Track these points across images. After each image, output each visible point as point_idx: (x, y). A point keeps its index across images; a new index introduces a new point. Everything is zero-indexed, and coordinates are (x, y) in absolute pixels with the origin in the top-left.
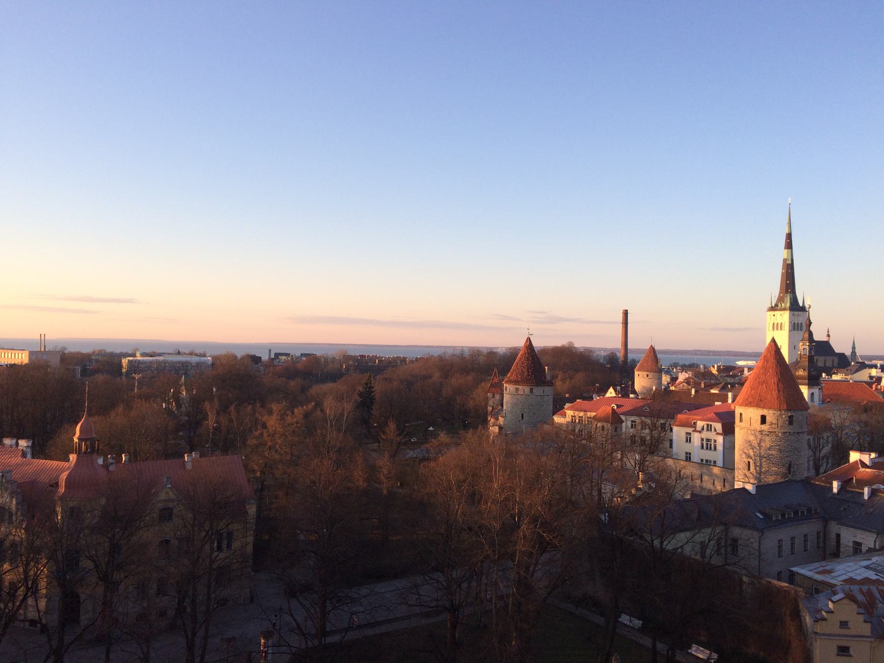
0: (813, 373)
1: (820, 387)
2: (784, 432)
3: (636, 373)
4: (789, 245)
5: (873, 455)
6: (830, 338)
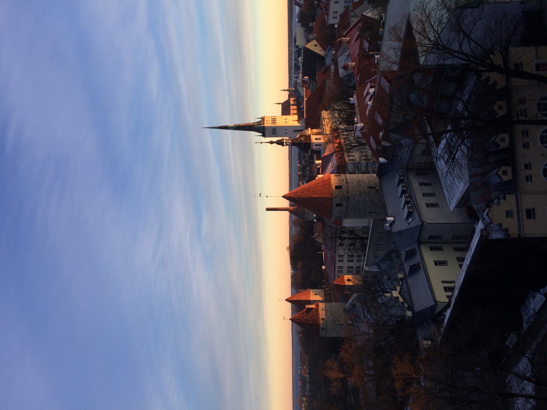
1: (311, 135)
2: (347, 192)
3: (306, 220)
6: (280, 102)
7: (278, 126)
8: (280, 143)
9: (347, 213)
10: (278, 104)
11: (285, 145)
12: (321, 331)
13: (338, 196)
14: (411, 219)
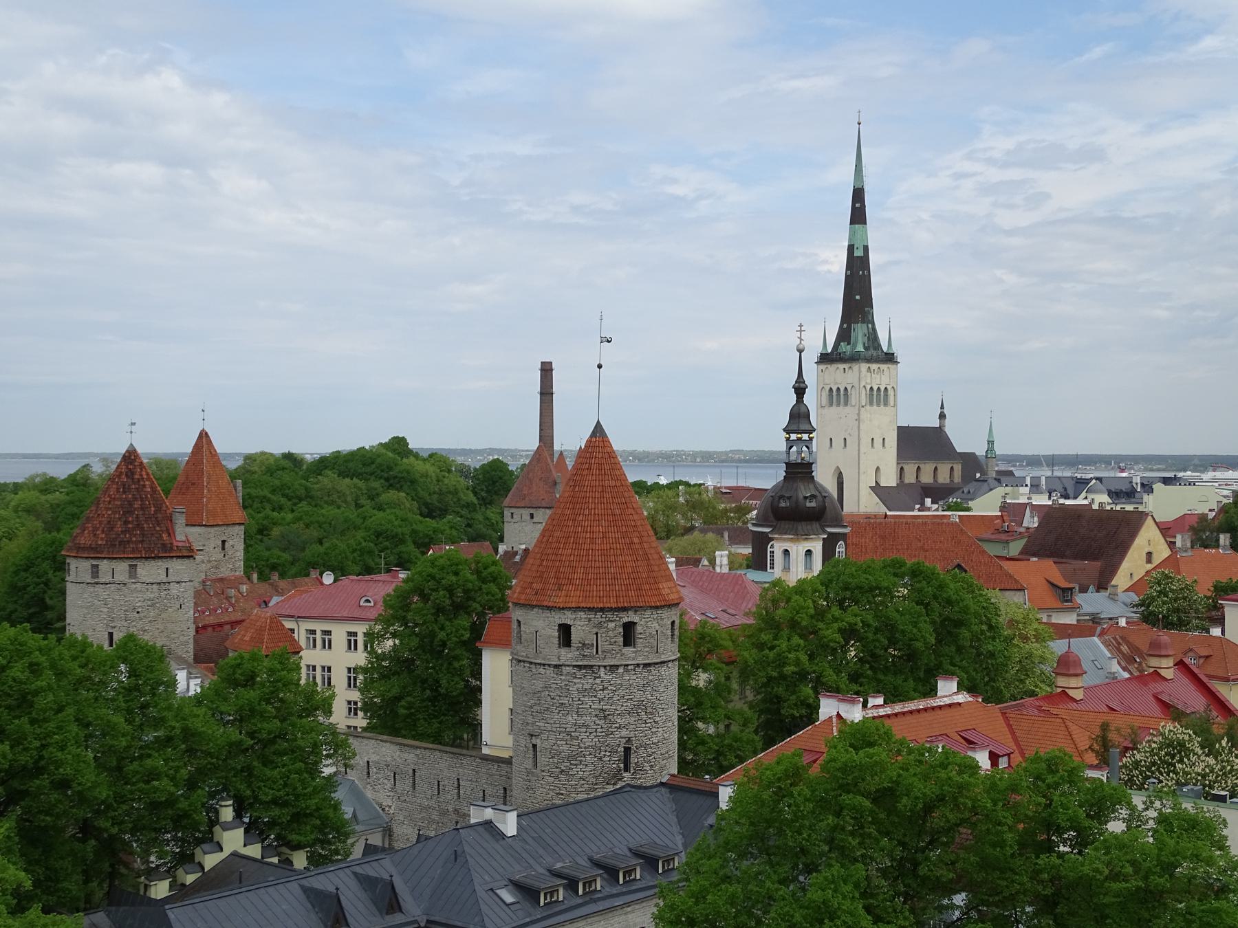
0: (808, 504)
2: (611, 666)
3: (507, 513)
4: (858, 216)
5: (872, 702)
6: (947, 422)
7: (859, 415)
8: (799, 419)
9: (535, 664)
10: (942, 416)
11: (788, 439)
12: (87, 564)
13: (597, 634)
14: (508, 897)
